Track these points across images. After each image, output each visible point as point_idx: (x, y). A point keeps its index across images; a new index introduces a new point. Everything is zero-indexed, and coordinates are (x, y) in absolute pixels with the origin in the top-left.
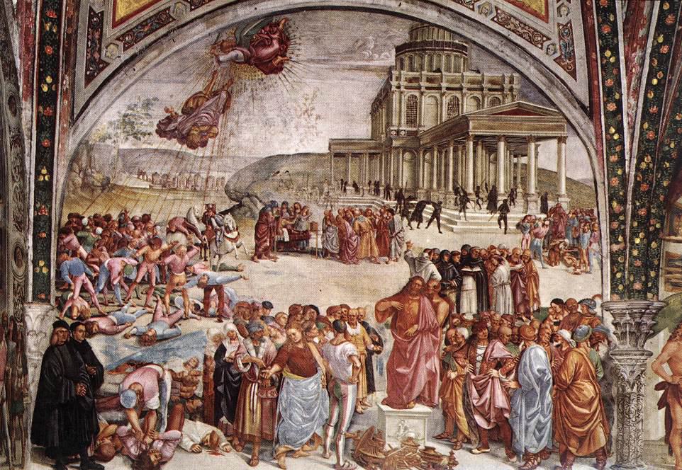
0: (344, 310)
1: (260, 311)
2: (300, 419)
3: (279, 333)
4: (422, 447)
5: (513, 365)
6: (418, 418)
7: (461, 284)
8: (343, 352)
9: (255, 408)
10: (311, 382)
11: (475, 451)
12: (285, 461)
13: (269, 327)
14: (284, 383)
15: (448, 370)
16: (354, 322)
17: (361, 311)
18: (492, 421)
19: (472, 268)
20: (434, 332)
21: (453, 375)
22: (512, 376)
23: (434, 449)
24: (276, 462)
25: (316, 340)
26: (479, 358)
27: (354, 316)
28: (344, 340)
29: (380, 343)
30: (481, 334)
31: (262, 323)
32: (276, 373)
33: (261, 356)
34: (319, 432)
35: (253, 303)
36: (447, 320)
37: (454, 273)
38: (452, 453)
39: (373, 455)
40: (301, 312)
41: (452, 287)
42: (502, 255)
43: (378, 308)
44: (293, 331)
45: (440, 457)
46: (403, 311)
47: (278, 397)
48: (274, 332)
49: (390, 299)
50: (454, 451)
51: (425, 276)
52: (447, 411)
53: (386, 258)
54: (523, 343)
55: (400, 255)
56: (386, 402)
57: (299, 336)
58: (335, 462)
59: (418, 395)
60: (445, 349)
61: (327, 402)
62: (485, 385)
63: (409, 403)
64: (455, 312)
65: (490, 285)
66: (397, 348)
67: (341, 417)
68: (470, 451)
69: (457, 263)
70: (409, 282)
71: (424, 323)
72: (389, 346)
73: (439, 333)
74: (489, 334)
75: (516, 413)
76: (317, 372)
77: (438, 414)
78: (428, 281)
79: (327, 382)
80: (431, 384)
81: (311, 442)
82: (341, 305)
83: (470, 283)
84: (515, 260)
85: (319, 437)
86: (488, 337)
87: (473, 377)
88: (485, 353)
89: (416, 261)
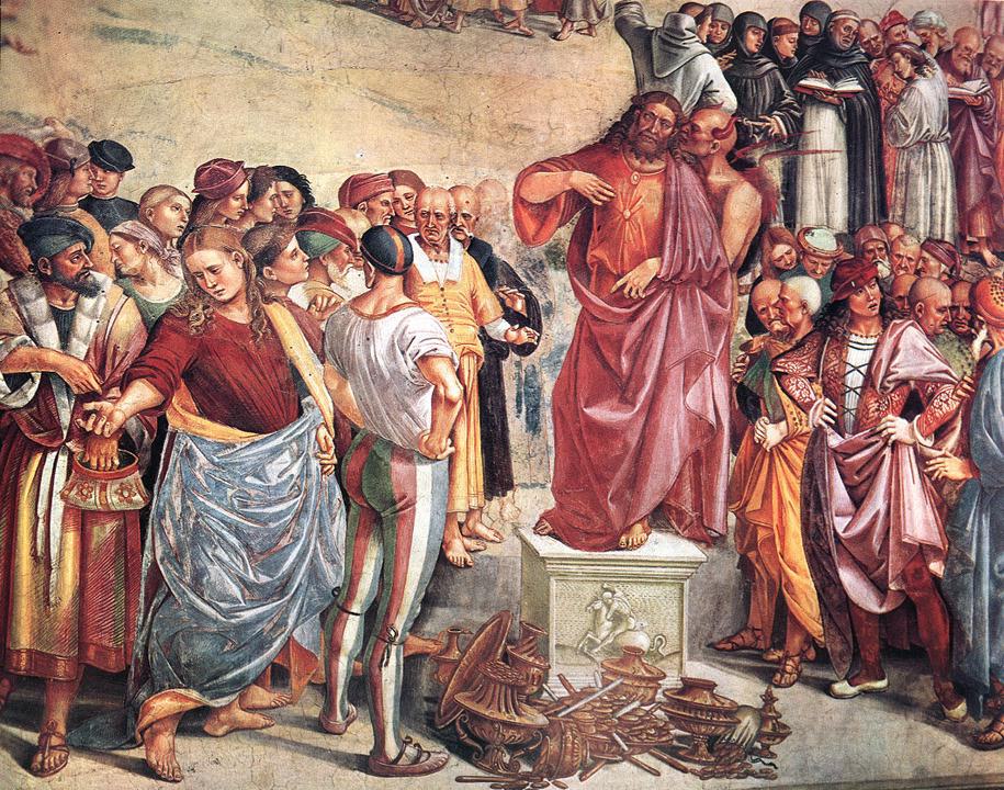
0: (402, 190)
1: (82, 175)
2: (235, 591)
3: (154, 265)
4: (672, 681)
5: (954, 405)
6: (659, 581)
7: (798, 127)
8: (400, 345)
9: (54, 551)
10: (277, 451)
11: (842, 687)
12: (173, 750)
13: (116, 239)
14: (174, 455)
15: (757, 415)
16: (439, 238)
17: (463, 197)
18: (893, 587)
19: (833, 78)
20: (713, 287)
21: (772, 434)
22: (952, 440)
23: (710, 686)
24: (138, 753)
25: (298, 295)
26: (855, 379)
27: (437, 215)
28: (404, 299)
29: (531, 317)
30: (860, 298)
31: (88, 221)
32: (142, 414)
33: (80, 348)
34: (306, 634)
35: (54, 145)
36: (755, 247)
37: (779, 93)
38: (769, 699)
39: (505, 717)
40: (244, 190)
41: (769, 139)
42: (923, 47)
43: (524, 194)
44: (207, 257)
45: (733, 712)
46: (608, 207)
47: (147, 509)
48: (133, 259)
49: (566, 162)
50: (777, 692)
51: (686, 93)
52: (752, 555)
53: (555, 20)
54: (982, 335)
55: (600, 15)
56: (555, 525)
57: (232, 277)
58: (365, 749)
59: (657, 499)
60: (745, 346)
61: (339, 528)
62: (872, 468)
63: (628, 529)
64: (778, 223)
65: (888, 139)
66: (590, 333)
67: (388, 580)
68: (826, 688)
69: (788, 58)
70: (632, 109)
71: (678, 251)
72: (561, 327)
73: (727, 292)
74: (883, 301)
75: (963, 559)
76: (300, 413)
77: (726, 568)
78: (692, 115)
79: (340, 453)
80: (700, 460)
81: (277, 675)
82: (391, 174)
83: (825, 129)
84: (963, 66)
85: (306, 655)
86: (883, 311)
87: (834, 440)
88: (870, 364)
89: (655, 43)
